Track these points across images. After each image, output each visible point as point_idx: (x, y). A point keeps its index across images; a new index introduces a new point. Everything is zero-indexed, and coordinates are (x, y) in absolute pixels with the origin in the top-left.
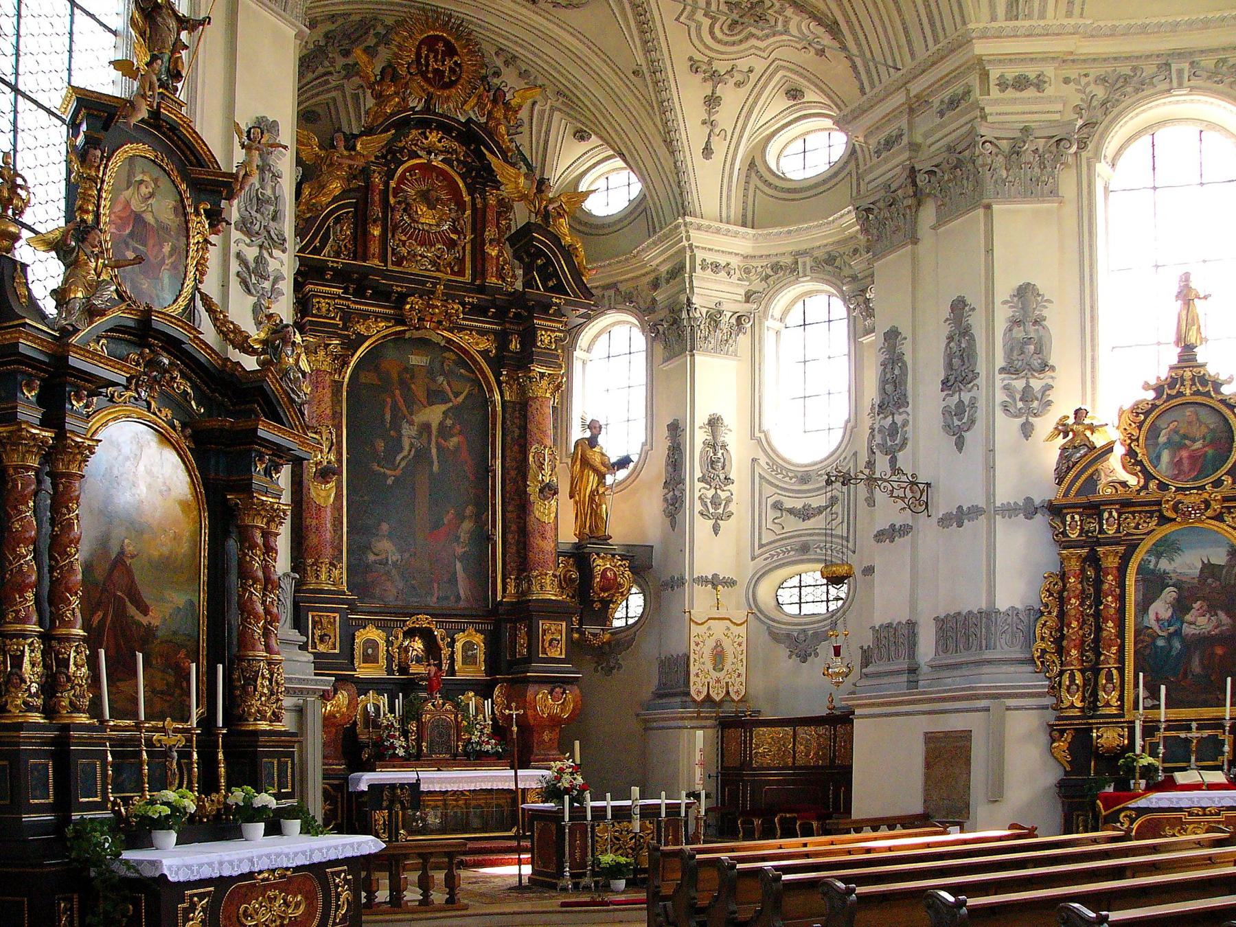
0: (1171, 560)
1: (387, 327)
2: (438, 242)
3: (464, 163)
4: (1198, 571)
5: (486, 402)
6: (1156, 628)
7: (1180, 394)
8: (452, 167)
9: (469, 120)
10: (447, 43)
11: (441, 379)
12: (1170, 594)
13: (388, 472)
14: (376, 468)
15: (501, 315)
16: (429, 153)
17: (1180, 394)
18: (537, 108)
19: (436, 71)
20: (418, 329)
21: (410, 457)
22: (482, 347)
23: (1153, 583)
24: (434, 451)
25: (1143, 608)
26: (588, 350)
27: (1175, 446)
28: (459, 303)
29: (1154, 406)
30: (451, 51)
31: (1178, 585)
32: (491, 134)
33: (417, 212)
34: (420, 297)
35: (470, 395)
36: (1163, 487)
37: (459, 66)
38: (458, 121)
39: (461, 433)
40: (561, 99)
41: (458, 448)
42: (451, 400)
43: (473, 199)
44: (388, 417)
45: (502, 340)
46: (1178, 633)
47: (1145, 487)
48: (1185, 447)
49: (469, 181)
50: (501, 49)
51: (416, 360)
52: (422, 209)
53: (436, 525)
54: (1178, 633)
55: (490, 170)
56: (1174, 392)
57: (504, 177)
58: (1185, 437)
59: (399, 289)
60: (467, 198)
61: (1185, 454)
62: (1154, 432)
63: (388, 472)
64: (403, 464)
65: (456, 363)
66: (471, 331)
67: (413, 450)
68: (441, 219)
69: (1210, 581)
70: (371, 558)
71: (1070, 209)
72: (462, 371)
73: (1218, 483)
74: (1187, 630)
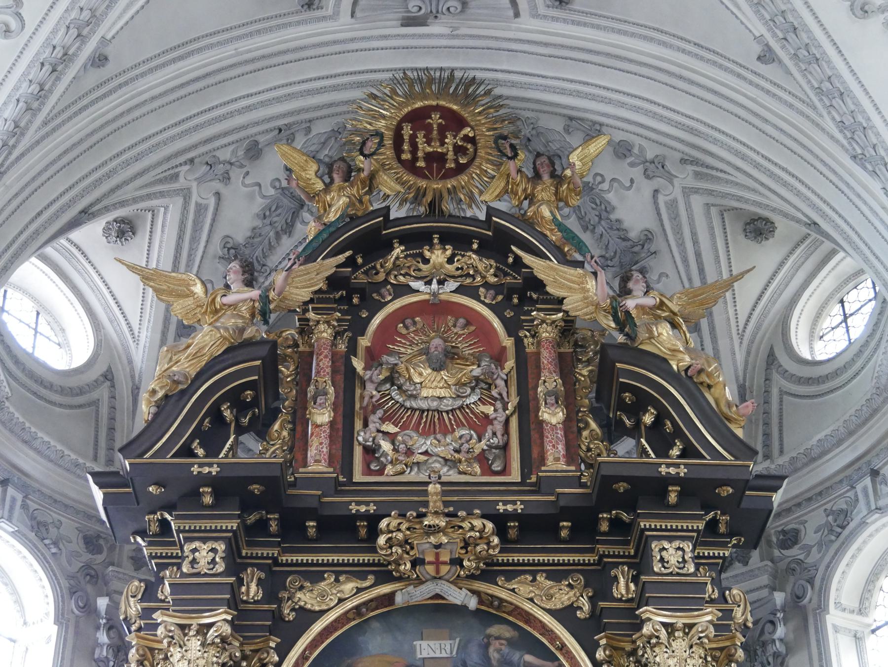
1: (359, 590)
2: (460, 425)
3: (497, 288)
8: (477, 298)
9: (491, 212)
10: (447, 113)
16: (429, 283)
18: (661, 199)
19: (429, 157)
20: (419, 582)
22: (563, 597)
26: (862, 610)
28: (484, 516)
30: (455, 121)
32: (528, 223)
33: (410, 379)
34: (403, 515)
37: (472, 141)
38: (474, 221)
40: (690, 168)
43: (519, 344)
49: (509, 314)
50: (571, 119)
55: (539, 285)
57: (562, 286)
59: (363, 509)
60: (508, 342)
65: (511, 643)
66: (534, 574)
68: (460, 384)
72: (529, 658)
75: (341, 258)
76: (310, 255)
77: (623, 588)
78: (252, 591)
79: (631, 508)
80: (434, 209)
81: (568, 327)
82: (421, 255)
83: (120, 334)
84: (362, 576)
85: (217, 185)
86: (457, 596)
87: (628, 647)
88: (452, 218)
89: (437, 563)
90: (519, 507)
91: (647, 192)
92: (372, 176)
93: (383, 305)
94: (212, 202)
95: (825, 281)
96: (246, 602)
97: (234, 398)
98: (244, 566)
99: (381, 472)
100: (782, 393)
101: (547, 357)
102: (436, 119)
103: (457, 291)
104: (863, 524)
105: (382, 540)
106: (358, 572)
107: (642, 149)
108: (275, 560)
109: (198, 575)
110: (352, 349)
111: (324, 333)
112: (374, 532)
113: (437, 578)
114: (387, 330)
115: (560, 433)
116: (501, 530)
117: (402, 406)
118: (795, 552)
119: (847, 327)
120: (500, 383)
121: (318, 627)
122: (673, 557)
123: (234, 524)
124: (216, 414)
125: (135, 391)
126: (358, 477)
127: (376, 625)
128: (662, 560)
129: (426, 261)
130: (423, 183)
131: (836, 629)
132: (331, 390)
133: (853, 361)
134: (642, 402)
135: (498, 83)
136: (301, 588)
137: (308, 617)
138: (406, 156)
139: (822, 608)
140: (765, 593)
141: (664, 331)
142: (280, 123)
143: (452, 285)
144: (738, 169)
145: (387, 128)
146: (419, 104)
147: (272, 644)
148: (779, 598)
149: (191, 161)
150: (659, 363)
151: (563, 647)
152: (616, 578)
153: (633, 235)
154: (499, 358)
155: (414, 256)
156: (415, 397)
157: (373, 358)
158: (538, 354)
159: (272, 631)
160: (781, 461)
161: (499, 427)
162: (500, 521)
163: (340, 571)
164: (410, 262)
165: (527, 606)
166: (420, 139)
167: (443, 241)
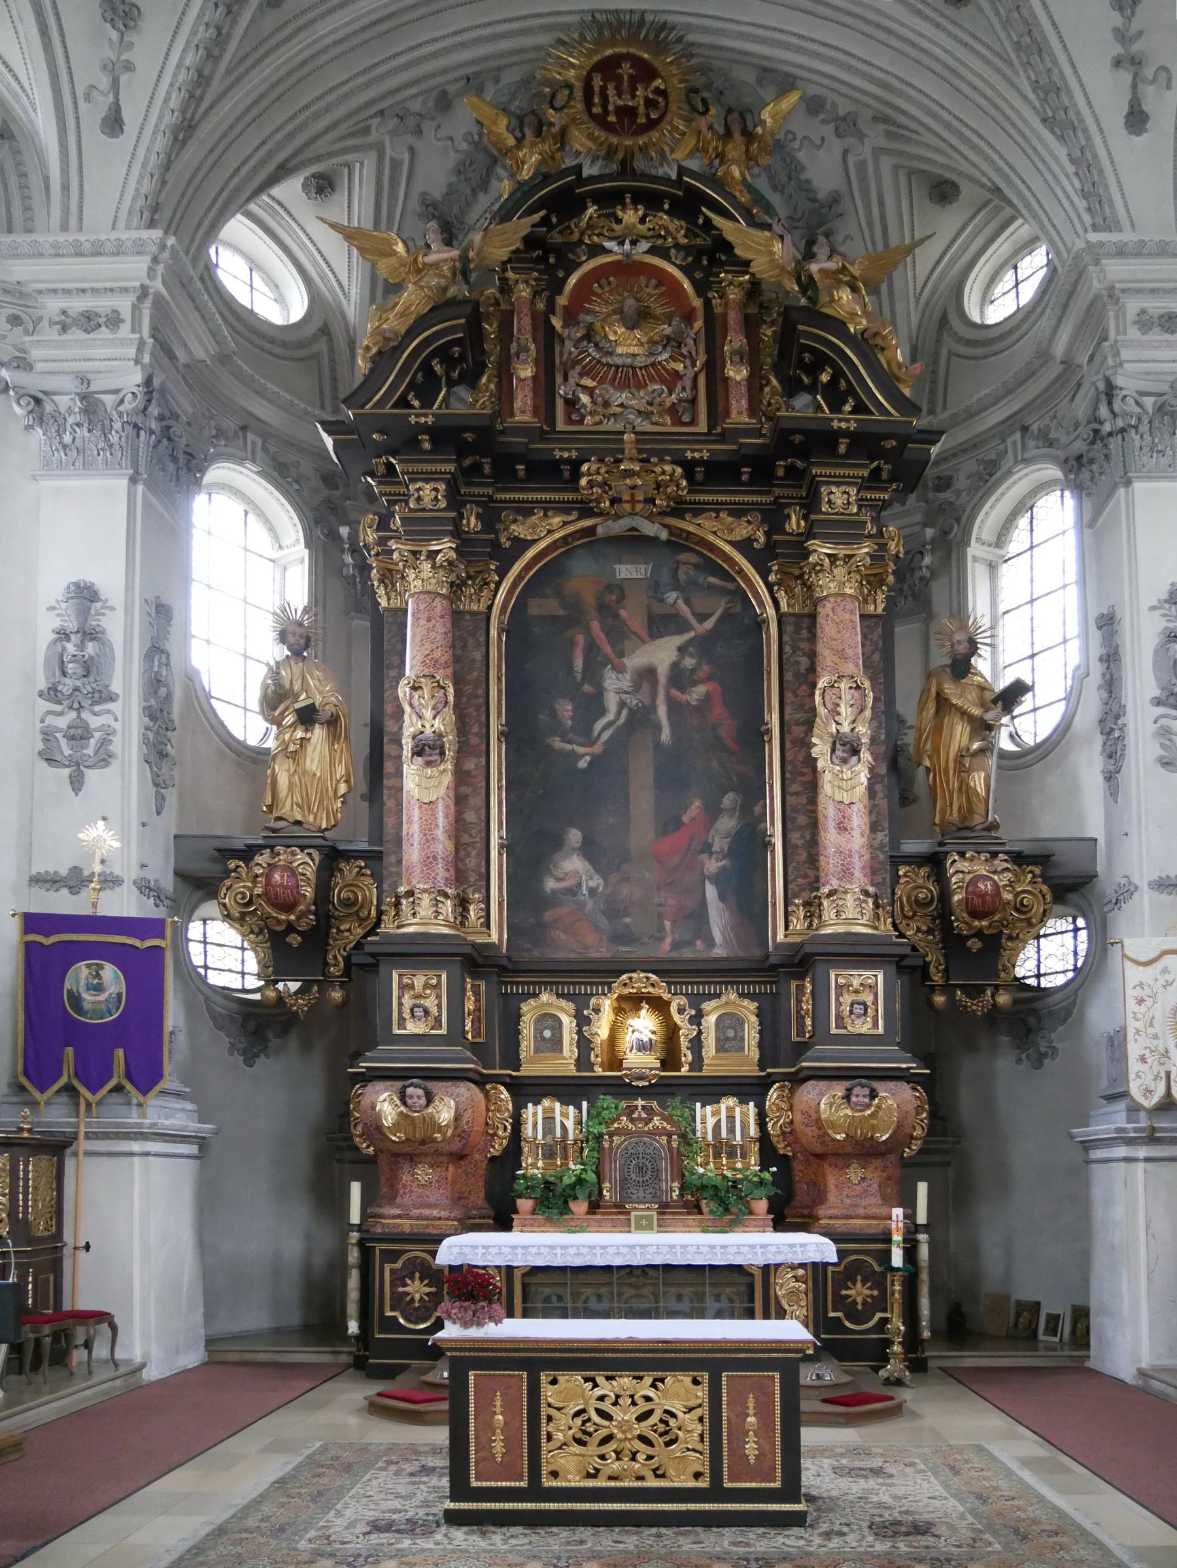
1: (565, 523)
3: (687, 250)
5: (760, 624)
8: (667, 258)
9: (682, 171)
10: (637, 62)
11: (672, 596)
13: (580, 750)
14: (558, 744)
15: (763, 474)
16: (622, 243)
19: (621, 110)
20: (617, 517)
21: (621, 721)
22: (742, 531)
24: (662, 710)
28: (674, 462)
30: (646, 72)
32: (719, 184)
33: (606, 337)
35: (726, 617)
37: (663, 93)
38: (665, 180)
39: (709, 679)
41: (708, 697)
42: (689, 628)
43: (708, 304)
44: (579, 663)
45: (774, 518)
49: (698, 275)
51: (626, 571)
52: (616, 331)
53: (669, 823)
55: (728, 247)
57: (749, 248)
59: (566, 455)
60: (697, 303)
63: (580, 750)
64: (606, 735)
65: (696, 567)
66: (717, 511)
67: (625, 712)
68: (652, 342)
70: (550, 884)
72: (711, 579)
75: (536, 217)
76: (505, 215)
77: (795, 523)
78: (472, 523)
79: (805, 457)
80: (626, 168)
81: (754, 289)
82: (615, 215)
83: (332, 291)
84: (567, 511)
85: (410, 139)
86: (650, 529)
87: (797, 572)
88: (645, 177)
89: (633, 501)
90: (706, 455)
92: (564, 132)
93: (578, 265)
94: (406, 156)
95: (1001, 247)
96: (468, 532)
97: (443, 353)
98: (463, 504)
99: (581, 422)
100: (950, 353)
101: (733, 318)
102: (626, 69)
103: (652, 251)
104: (1009, 473)
105: (583, 482)
106: (564, 508)
107: (834, 103)
108: (490, 498)
109: (424, 510)
110: (551, 308)
111: (524, 292)
112: (576, 475)
113: (633, 514)
114: (583, 291)
115: (744, 389)
116: (689, 474)
117: (599, 362)
118: (948, 495)
119: (1017, 293)
120: (690, 342)
121: (530, 553)
122: (839, 499)
123: (451, 468)
124: (426, 368)
125: (352, 344)
126: (561, 426)
127: (580, 552)
128: (829, 502)
129: (619, 221)
130: (615, 140)
131: (975, 559)
132: (533, 347)
133: (1019, 326)
134: (821, 361)
135: (690, 27)
136: (515, 521)
137: (524, 545)
138: (597, 110)
139: (965, 542)
140: (917, 528)
142: (469, 70)
143: (644, 246)
144: (928, 129)
145: (577, 78)
146: (609, 52)
147: (493, 567)
148: (929, 533)
149: (381, 113)
150: (837, 326)
151: (741, 572)
152: (789, 517)
153: (822, 195)
154: (689, 318)
155: (607, 216)
156: (610, 354)
157: (570, 317)
158: (725, 316)
159: (492, 556)
160: (945, 416)
161: (688, 382)
162: (689, 467)
163: (548, 508)
164: (603, 222)
165: (711, 538)
166: (611, 92)
167: (635, 202)
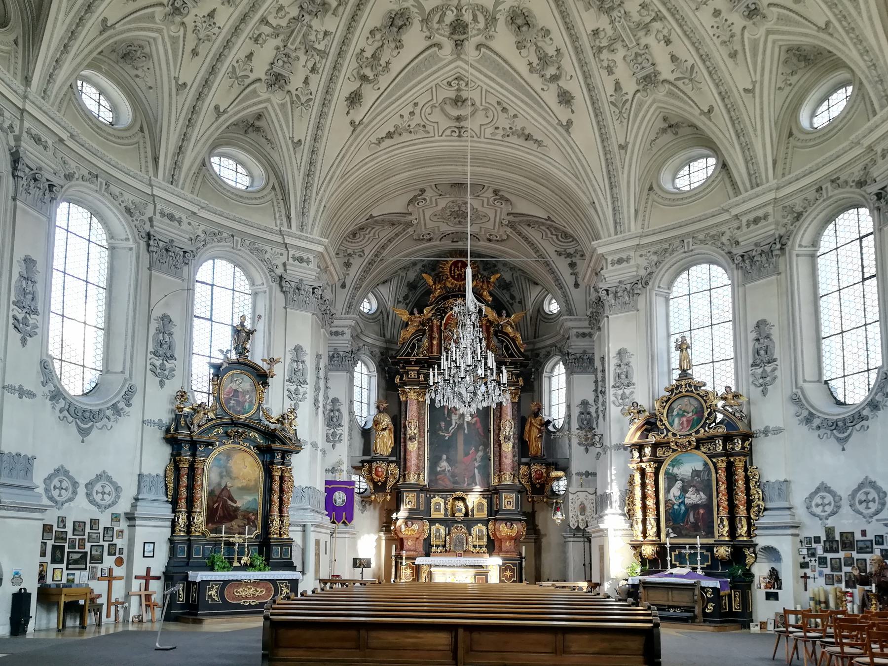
0: (679, 468)
4: (690, 474)
6: (674, 500)
7: (681, 392)
12: (679, 484)
17: (681, 392)
23: (672, 479)
25: (668, 490)
27: (681, 416)
29: (669, 399)
31: (682, 480)
36: (674, 435)
46: (683, 502)
47: (667, 435)
48: (684, 416)
54: (683, 502)
56: (678, 391)
58: (684, 411)
61: (684, 419)
62: (670, 410)
69: (696, 478)
71: (642, 313)
73: (697, 432)
74: (687, 501)
91: (511, 273)
141: (509, 328)
150: (507, 334)
